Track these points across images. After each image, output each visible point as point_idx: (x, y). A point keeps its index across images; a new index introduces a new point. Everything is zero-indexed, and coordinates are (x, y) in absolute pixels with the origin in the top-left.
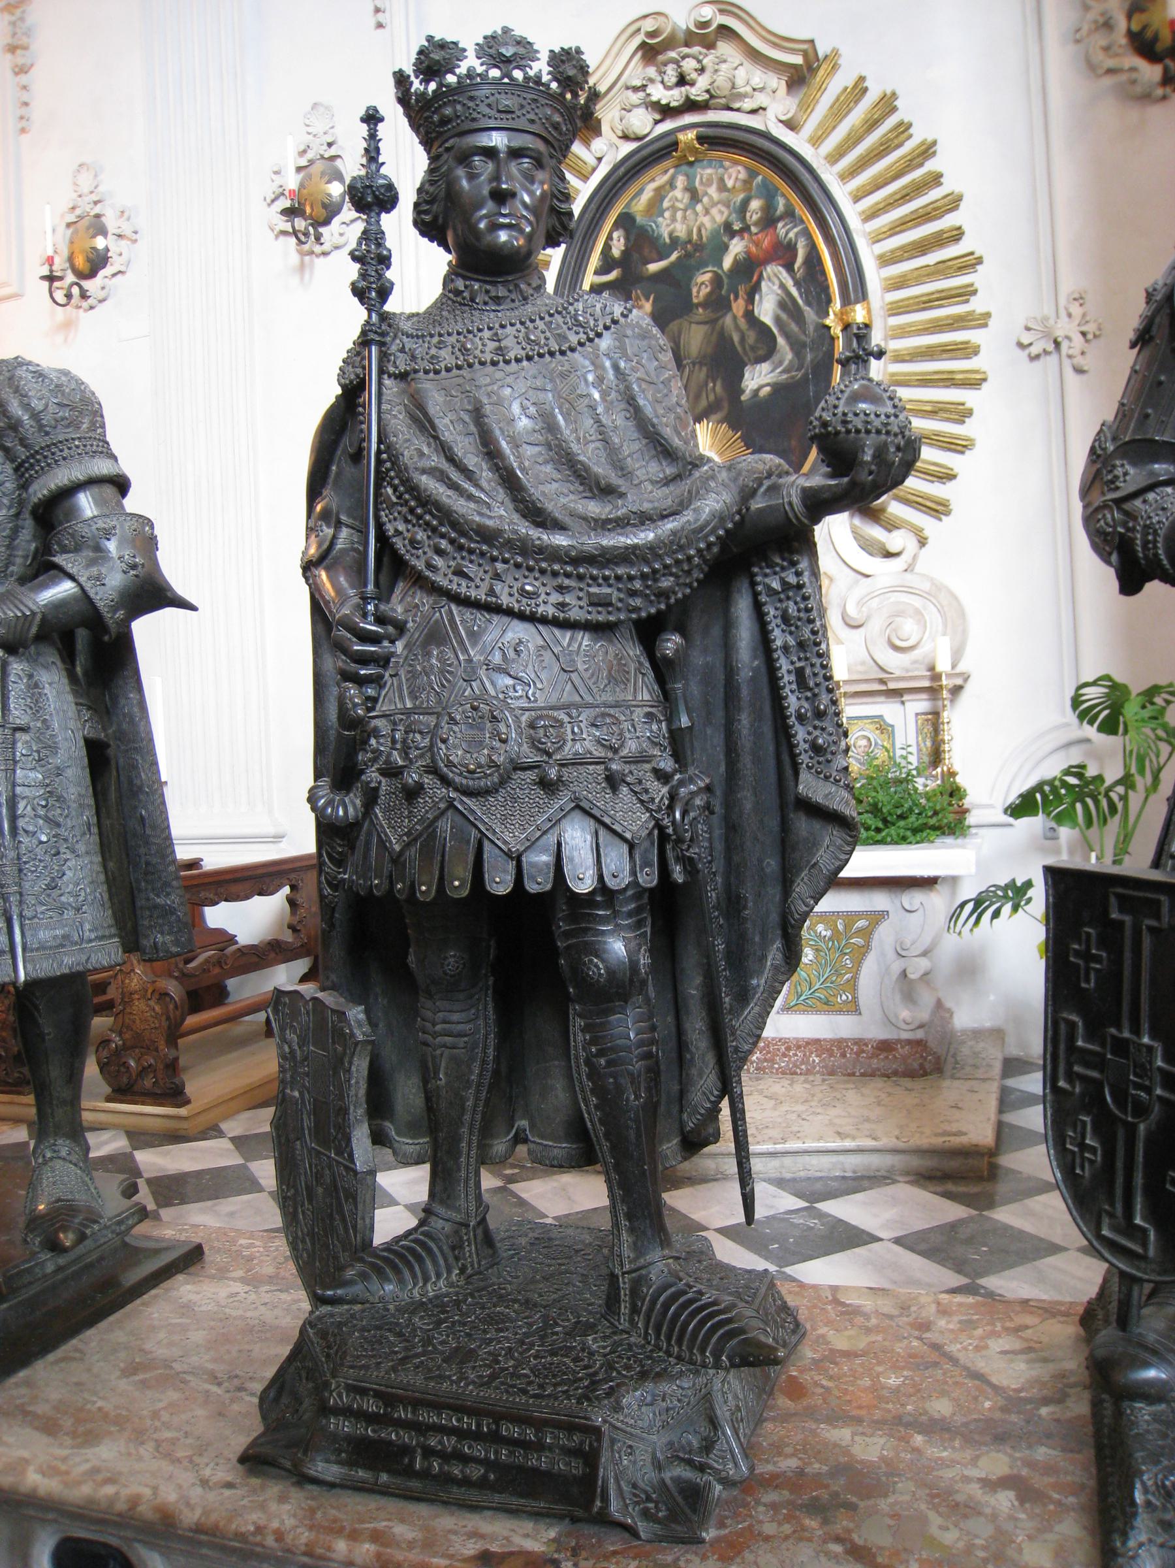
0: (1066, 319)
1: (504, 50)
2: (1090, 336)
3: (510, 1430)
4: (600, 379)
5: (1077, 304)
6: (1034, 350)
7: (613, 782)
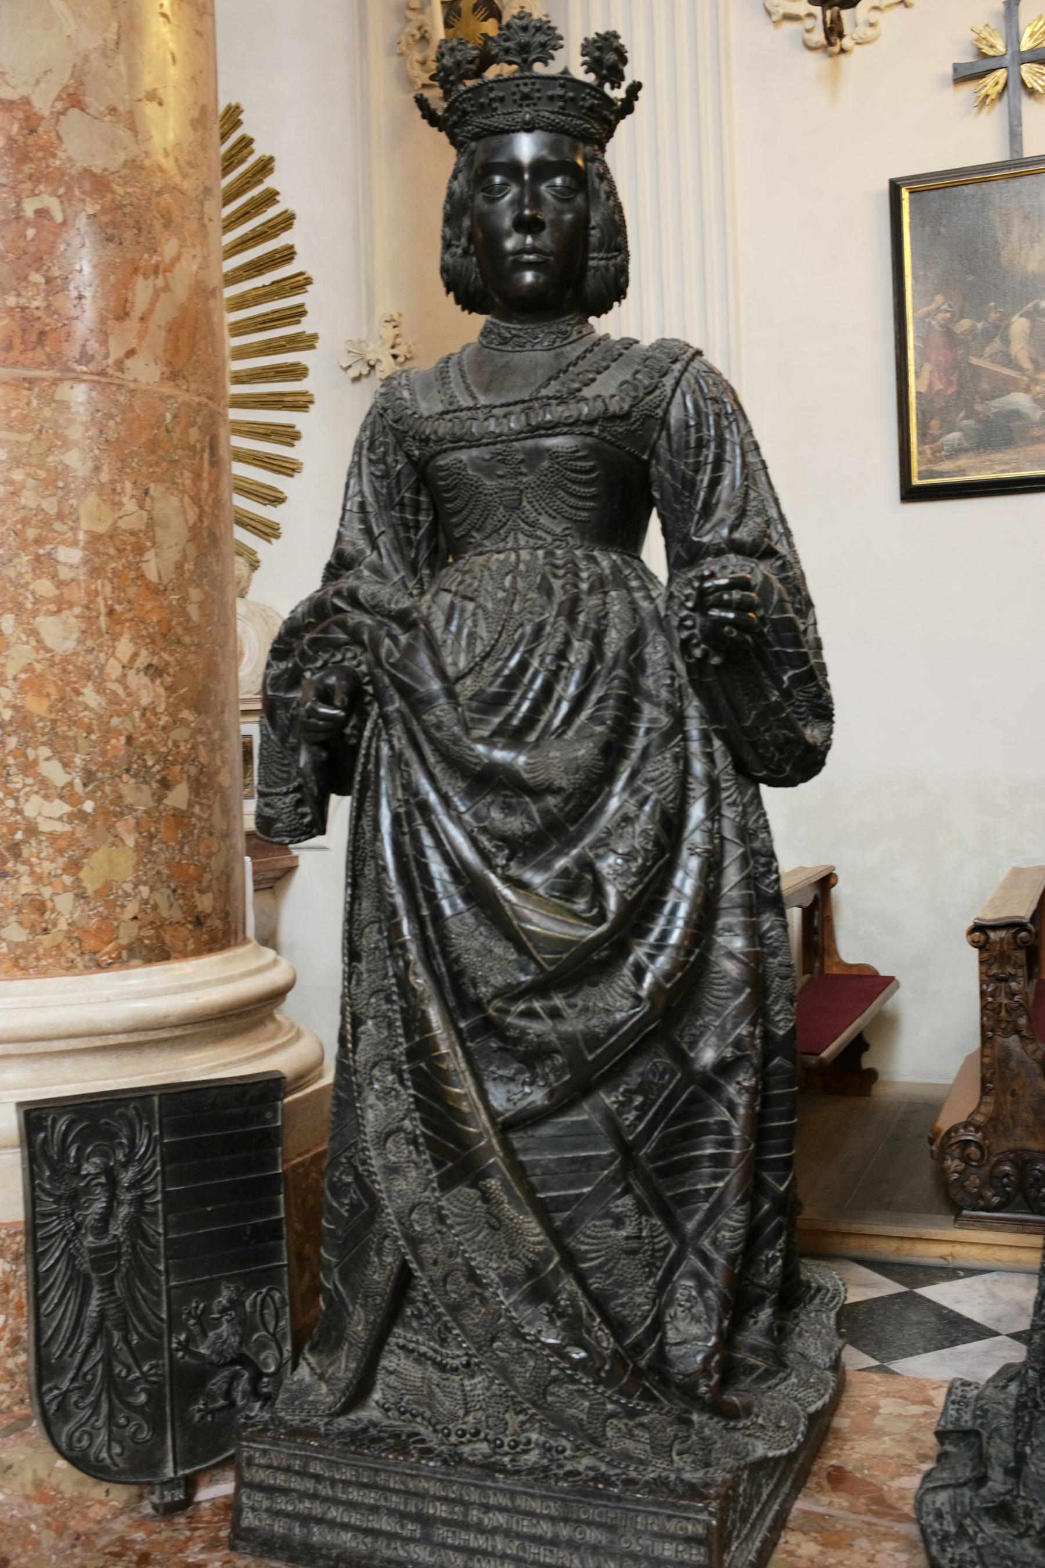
0: (380, 342)
2: (401, 359)
5: (390, 326)
6: (354, 373)
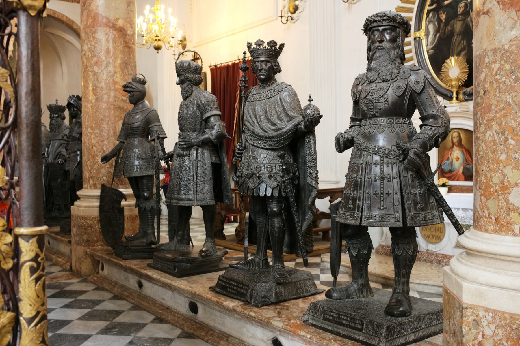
1: (259, 43)
3: (240, 285)
4: (278, 102)
7: (270, 177)
